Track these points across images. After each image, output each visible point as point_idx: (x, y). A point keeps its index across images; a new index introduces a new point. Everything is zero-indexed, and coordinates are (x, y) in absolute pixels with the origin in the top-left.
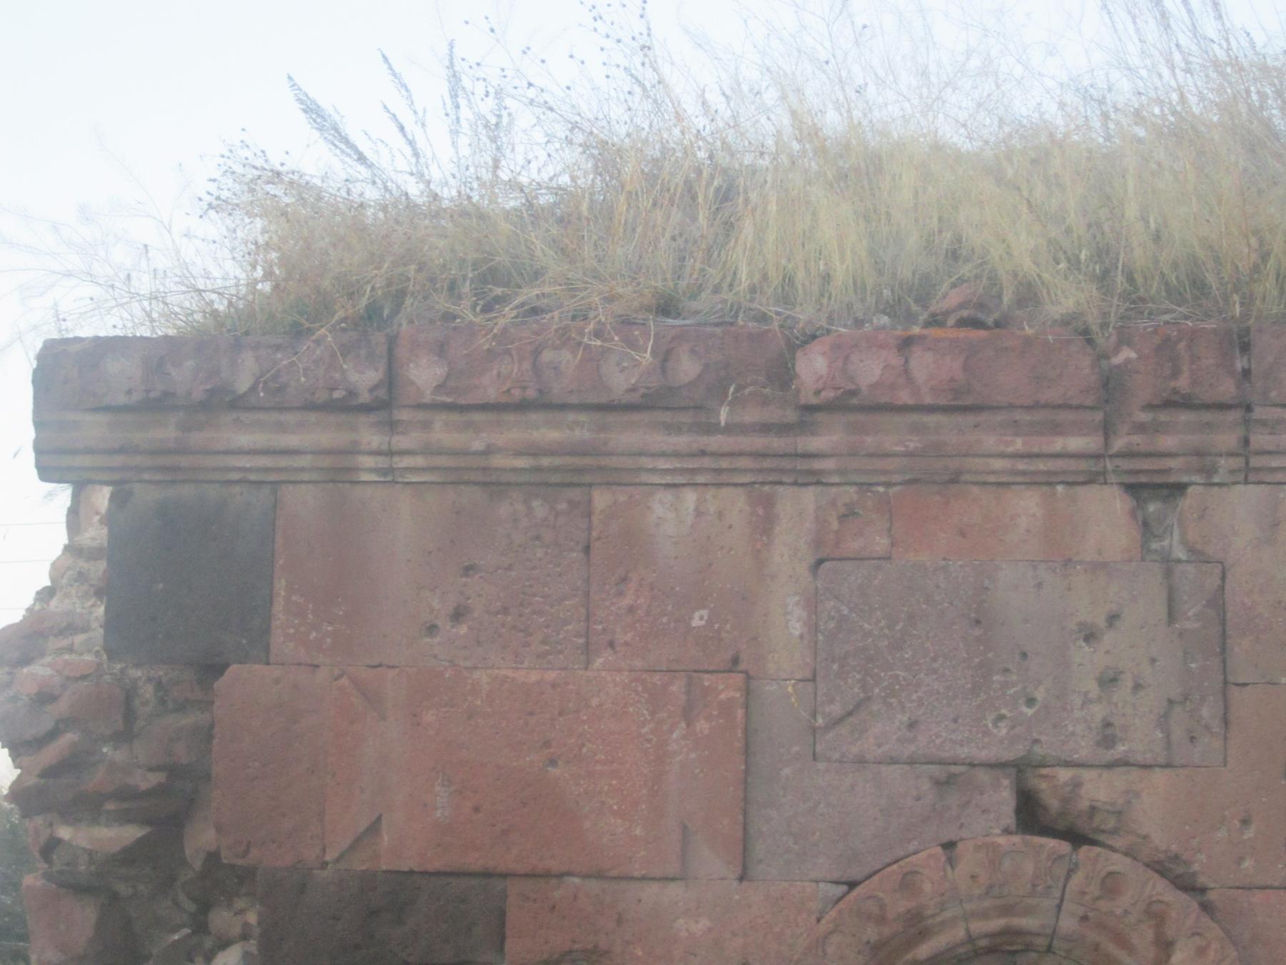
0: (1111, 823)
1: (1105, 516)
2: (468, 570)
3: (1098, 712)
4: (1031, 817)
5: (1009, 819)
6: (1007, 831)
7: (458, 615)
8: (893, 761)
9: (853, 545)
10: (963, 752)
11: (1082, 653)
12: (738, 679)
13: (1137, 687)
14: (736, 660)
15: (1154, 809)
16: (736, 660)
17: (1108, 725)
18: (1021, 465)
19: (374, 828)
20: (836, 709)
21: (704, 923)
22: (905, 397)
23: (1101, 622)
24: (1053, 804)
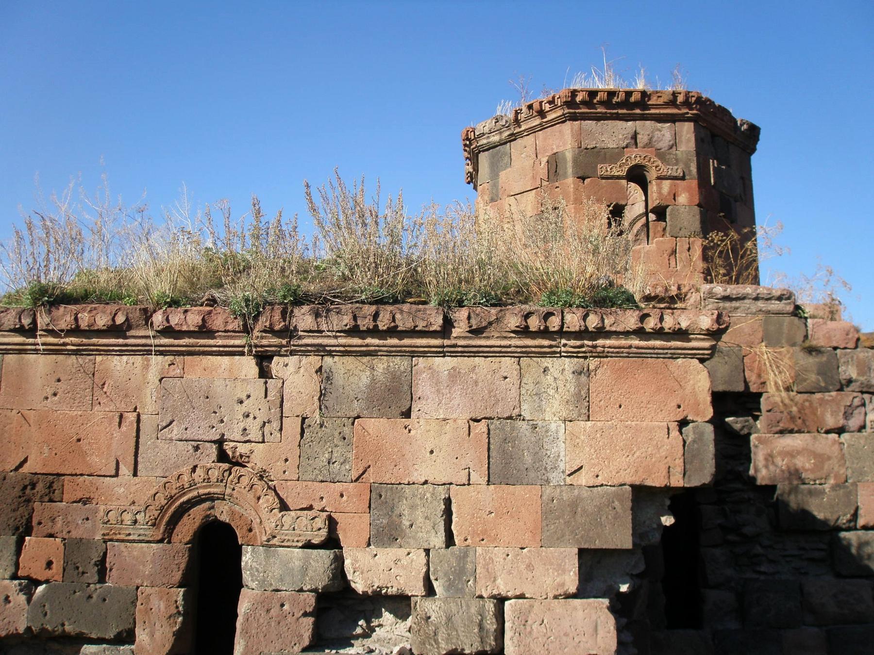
0: (247, 460)
1: (248, 366)
2: (59, 380)
3: (242, 425)
4: (222, 456)
5: (214, 457)
6: (213, 462)
7: (55, 395)
8: (181, 440)
9: (172, 374)
10: (200, 438)
11: (238, 407)
12: (135, 414)
13: (255, 418)
14: (136, 408)
15: (259, 455)
16: (136, 408)
17: (245, 430)
18: (221, 349)
19: (25, 460)
20: (164, 424)
21: (122, 490)
22: (185, 328)
23: (244, 398)
24: (230, 453)
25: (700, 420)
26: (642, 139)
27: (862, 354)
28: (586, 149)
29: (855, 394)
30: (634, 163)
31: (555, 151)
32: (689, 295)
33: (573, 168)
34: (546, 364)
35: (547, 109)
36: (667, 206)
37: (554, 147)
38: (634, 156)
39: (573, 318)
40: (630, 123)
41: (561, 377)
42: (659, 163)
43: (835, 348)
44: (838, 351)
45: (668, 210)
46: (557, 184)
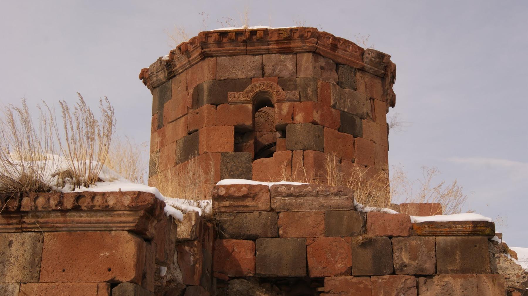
25: (124, 280)
26: (268, 70)
27: (414, 242)
28: (220, 80)
29: (407, 277)
30: (257, 90)
31: (197, 84)
32: (261, 194)
33: (208, 96)
34: (11, 239)
35: (192, 49)
36: (287, 124)
37: (197, 80)
38: (259, 85)
39: (28, 201)
40: (258, 57)
41: (22, 248)
42: (280, 88)
43: (391, 237)
44: (393, 240)
45: (287, 127)
46: (197, 110)
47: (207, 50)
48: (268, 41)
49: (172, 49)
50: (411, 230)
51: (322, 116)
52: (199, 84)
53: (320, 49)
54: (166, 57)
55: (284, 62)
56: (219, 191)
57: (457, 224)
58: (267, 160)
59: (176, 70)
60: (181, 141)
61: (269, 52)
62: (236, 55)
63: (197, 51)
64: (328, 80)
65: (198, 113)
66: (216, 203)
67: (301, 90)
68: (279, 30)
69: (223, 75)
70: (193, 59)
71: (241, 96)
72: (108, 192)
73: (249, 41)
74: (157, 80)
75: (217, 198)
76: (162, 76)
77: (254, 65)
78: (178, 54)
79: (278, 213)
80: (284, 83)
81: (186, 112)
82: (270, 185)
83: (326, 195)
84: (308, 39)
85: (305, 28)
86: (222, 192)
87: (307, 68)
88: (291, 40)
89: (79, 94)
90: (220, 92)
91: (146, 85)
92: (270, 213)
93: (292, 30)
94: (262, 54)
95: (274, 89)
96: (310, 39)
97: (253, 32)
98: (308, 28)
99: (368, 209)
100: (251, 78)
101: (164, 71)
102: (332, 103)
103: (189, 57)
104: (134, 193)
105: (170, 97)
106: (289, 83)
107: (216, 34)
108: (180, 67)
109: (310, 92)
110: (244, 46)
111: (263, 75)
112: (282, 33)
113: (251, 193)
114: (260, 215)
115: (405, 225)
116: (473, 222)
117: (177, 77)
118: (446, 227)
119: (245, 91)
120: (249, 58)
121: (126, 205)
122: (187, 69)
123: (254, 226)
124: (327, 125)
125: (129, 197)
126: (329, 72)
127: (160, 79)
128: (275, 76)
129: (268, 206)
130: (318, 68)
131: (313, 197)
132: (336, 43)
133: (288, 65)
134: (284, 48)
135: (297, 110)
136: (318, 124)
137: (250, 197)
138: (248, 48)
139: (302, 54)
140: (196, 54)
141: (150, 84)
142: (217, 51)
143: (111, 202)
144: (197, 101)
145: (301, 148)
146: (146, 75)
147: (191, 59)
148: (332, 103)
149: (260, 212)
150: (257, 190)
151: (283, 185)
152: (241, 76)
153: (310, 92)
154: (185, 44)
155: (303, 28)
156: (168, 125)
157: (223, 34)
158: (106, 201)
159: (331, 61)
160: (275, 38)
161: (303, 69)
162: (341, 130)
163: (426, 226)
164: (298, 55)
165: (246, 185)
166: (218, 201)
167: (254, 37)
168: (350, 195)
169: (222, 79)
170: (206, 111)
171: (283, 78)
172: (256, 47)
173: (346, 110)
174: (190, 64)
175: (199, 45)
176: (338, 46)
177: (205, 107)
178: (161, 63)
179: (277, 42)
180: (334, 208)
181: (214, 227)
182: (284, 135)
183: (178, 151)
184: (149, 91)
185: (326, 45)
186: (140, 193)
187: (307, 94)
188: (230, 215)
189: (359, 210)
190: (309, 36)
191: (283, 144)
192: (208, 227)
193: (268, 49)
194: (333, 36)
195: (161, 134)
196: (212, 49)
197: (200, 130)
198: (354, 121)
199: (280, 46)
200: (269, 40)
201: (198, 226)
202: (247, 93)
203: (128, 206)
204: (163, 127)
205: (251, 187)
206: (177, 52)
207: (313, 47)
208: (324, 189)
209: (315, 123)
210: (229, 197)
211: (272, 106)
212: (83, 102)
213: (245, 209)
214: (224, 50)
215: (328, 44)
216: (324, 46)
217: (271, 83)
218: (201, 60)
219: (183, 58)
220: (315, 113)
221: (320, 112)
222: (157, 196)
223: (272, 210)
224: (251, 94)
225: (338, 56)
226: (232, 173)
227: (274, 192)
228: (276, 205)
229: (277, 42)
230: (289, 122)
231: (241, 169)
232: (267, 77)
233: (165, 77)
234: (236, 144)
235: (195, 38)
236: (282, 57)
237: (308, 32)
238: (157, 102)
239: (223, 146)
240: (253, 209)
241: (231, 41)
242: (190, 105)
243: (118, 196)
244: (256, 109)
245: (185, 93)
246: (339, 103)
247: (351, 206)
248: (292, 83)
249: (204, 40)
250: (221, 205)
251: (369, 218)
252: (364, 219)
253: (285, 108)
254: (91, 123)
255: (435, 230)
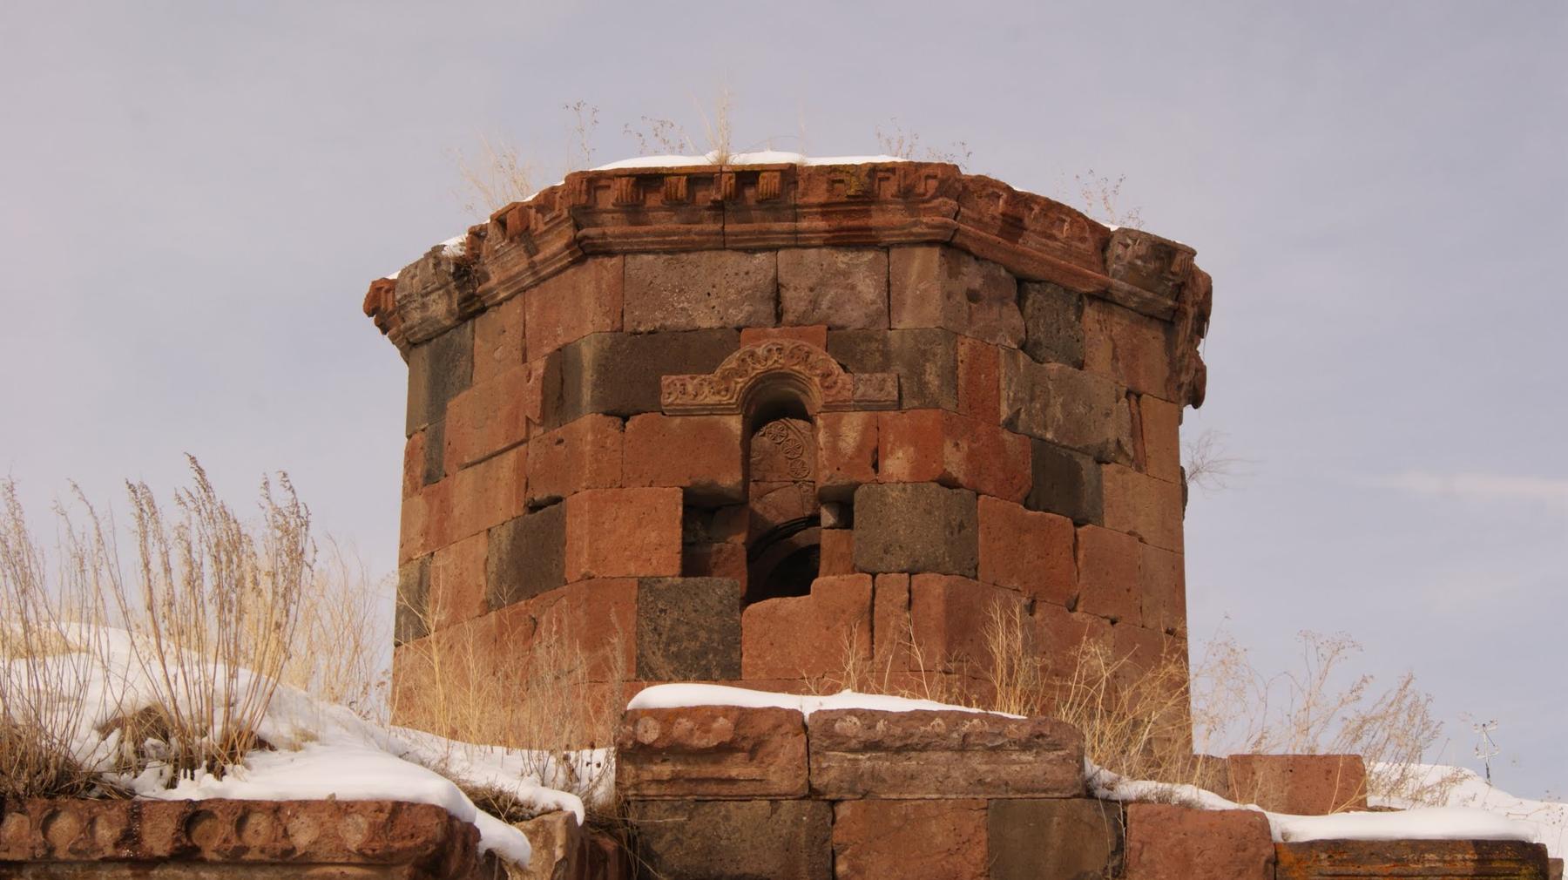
26: (795, 301)
28: (635, 333)
30: (760, 368)
31: (560, 342)
33: (595, 386)
37: (560, 330)
38: (766, 352)
42: (834, 365)
45: (858, 496)
46: (559, 432)
47: (592, 232)
48: (796, 206)
49: (476, 222)
50: (1271, 866)
51: (971, 457)
52: (566, 345)
53: (966, 235)
54: (454, 244)
55: (846, 274)
56: (640, 729)
57: (1423, 852)
58: (791, 603)
59: (491, 290)
60: (504, 532)
61: (798, 242)
62: (687, 251)
63: (560, 235)
64: (993, 337)
65: (560, 442)
66: (629, 768)
67: (903, 371)
68: (834, 169)
69: (647, 318)
70: (545, 260)
71: (706, 390)
72: (291, 803)
73: (737, 202)
74: (424, 320)
75: (631, 753)
76: (440, 308)
77: (750, 283)
78: (495, 241)
79: (833, 803)
80: (847, 346)
81: (523, 436)
82: (808, 705)
83: (994, 749)
84: (928, 201)
85: (920, 165)
86: (650, 733)
87: (922, 299)
88: (872, 202)
89: (193, 460)
90: (639, 370)
91: (384, 331)
92: (808, 805)
93: (874, 169)
94: (776, 249)
95: (813, 368)
96: (936, 202)
97: (748, 176)
98: (928, 165)
99: (1131, 788)
100: (739, 329)
101: (449, 293)
102: (1005, 412)
103: (532, 251)
104: (379, 806)
105: (467, 382)
106: (863, 347)
107: (624, 180)
108: (501, 283)
109: (932, 379)
110: (715, 220)
111: (779, 316)
112: (841, 181)
113: (744, 738)
114: (774, 811)
115: (1252, 850)
116: (1478, 844)
117: (492, 315)
118: (1390, 860)
119: (718, 372)
120: (731, 260)
121: (353, 847)
122: (524, 290)
123: (753, 847)
124: (989, 487)
125: (361, 820)
126: (996, 309)
127: (436, 315)
128: (820, 322)
129: (801, 781)
130: (960, 298)
131: (949, 754)
132: (1020, 212)
133: (860, 287)
134: (849, 229)
135: (891, 438)
136: (959, 486)
137: (742, 750)
138: (728, 228)
139: (907, 249)
140: (555, 245)
141: (399, 332)
142: (626, 236)
143: (303, 836)
144: (557, 399)
145: (904, 564)
146: (388, 303)
147: (537, 258)
148: (1005, 412)
149: (775, 800)
150: (766, 725)
151: (852, 712)
152: (706, 320)
153: (932, 379)
154: (521, 210)
155: (910, 163)
156: (460, 474)
157: (648, 180)
158: (286, 834)
159: (1003, 272)
160: (819, 195)
161: (909, 301)
162: (1032, 501)
163: (1323, 856)
164: (894, 253)
165: (727, 710)
166: (634, 763)
167: (750, 193)
168: (1071, 749)
169: (642, 329)
170: (590, 437)
171: (843, 328)
172: (755, 226)
173: (1049, 436)
174: (535, 273)
175: (565, 214)
176: (1027, 221)
177: (587, 425)
178: (437, 265)
179: (826, 210)
180: (1018, 791)
181: (620, 851)
182: (846, 520)
183: (494, 560)
184: (396, 351)
185: (987, 219)
186: (398, 809)
187: (923, 385)
188: (675, 810)
189: (1101, 792)
190: (931, 192)
191: (843, 548)
192: (605, 853)
193: (796, 232)
194: (1009, 189)
195: (436, 503)
196: (610, 230)
197: (570, 500)
198: (1074, 472)
199: (835, 224)
200: (799, 202)
201: (574, 863)
202: (725, 378)
203: (360, 852)
204: (443, 481)
205: (743, 715)
206: (493, 232)
207: (944, 226)
208: (987, 728)
209: (948, 482)
210: (673, 750)
211: (809, 419)
212: (207, 488)
213: (725, 790)
214: (647, 233)
215: (994, 218)
216: (979, 222)
217: (807, 345)
218: (573, 263)
219: (514, 254)
220: (948, 447)
221: (964, 445)
222: (454, 810)
223: (813, 793)
224: (740, 383)
225: (1024, 254)
226: (673, 649)
227: (819, 735)
228: (825, 779)
229: (826, 210)
230: (864, 479)
231: (703, 635)
232: (792, 324)
233: (450, 312)
234: (687, 546)
235: (553, 190)
236: (842, 259)
237: (928, 177)
238: (423, 393)
239: (645, 555)
240: (749, 789)
241: (673, 204)
242: (534, 412)
243: (325, 816)
244: (753, 426)
245: (519, 369)
246: (1029, 413)
247: (1075, 786)
248: (874, 346)
249: (584, 198)
250: (646, 776)
251: (1132, 826)
252: (1116, 827)
253: (852, 429)
254: (231, 546)
255: (1352, 869)
